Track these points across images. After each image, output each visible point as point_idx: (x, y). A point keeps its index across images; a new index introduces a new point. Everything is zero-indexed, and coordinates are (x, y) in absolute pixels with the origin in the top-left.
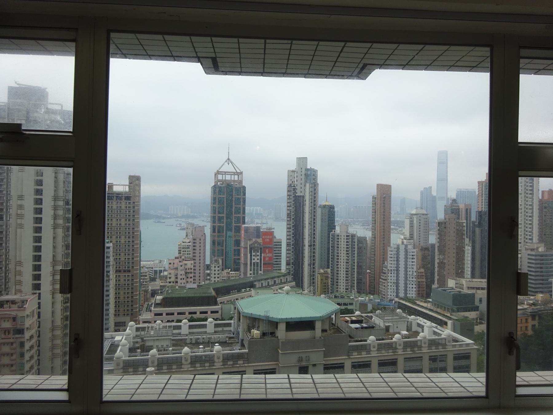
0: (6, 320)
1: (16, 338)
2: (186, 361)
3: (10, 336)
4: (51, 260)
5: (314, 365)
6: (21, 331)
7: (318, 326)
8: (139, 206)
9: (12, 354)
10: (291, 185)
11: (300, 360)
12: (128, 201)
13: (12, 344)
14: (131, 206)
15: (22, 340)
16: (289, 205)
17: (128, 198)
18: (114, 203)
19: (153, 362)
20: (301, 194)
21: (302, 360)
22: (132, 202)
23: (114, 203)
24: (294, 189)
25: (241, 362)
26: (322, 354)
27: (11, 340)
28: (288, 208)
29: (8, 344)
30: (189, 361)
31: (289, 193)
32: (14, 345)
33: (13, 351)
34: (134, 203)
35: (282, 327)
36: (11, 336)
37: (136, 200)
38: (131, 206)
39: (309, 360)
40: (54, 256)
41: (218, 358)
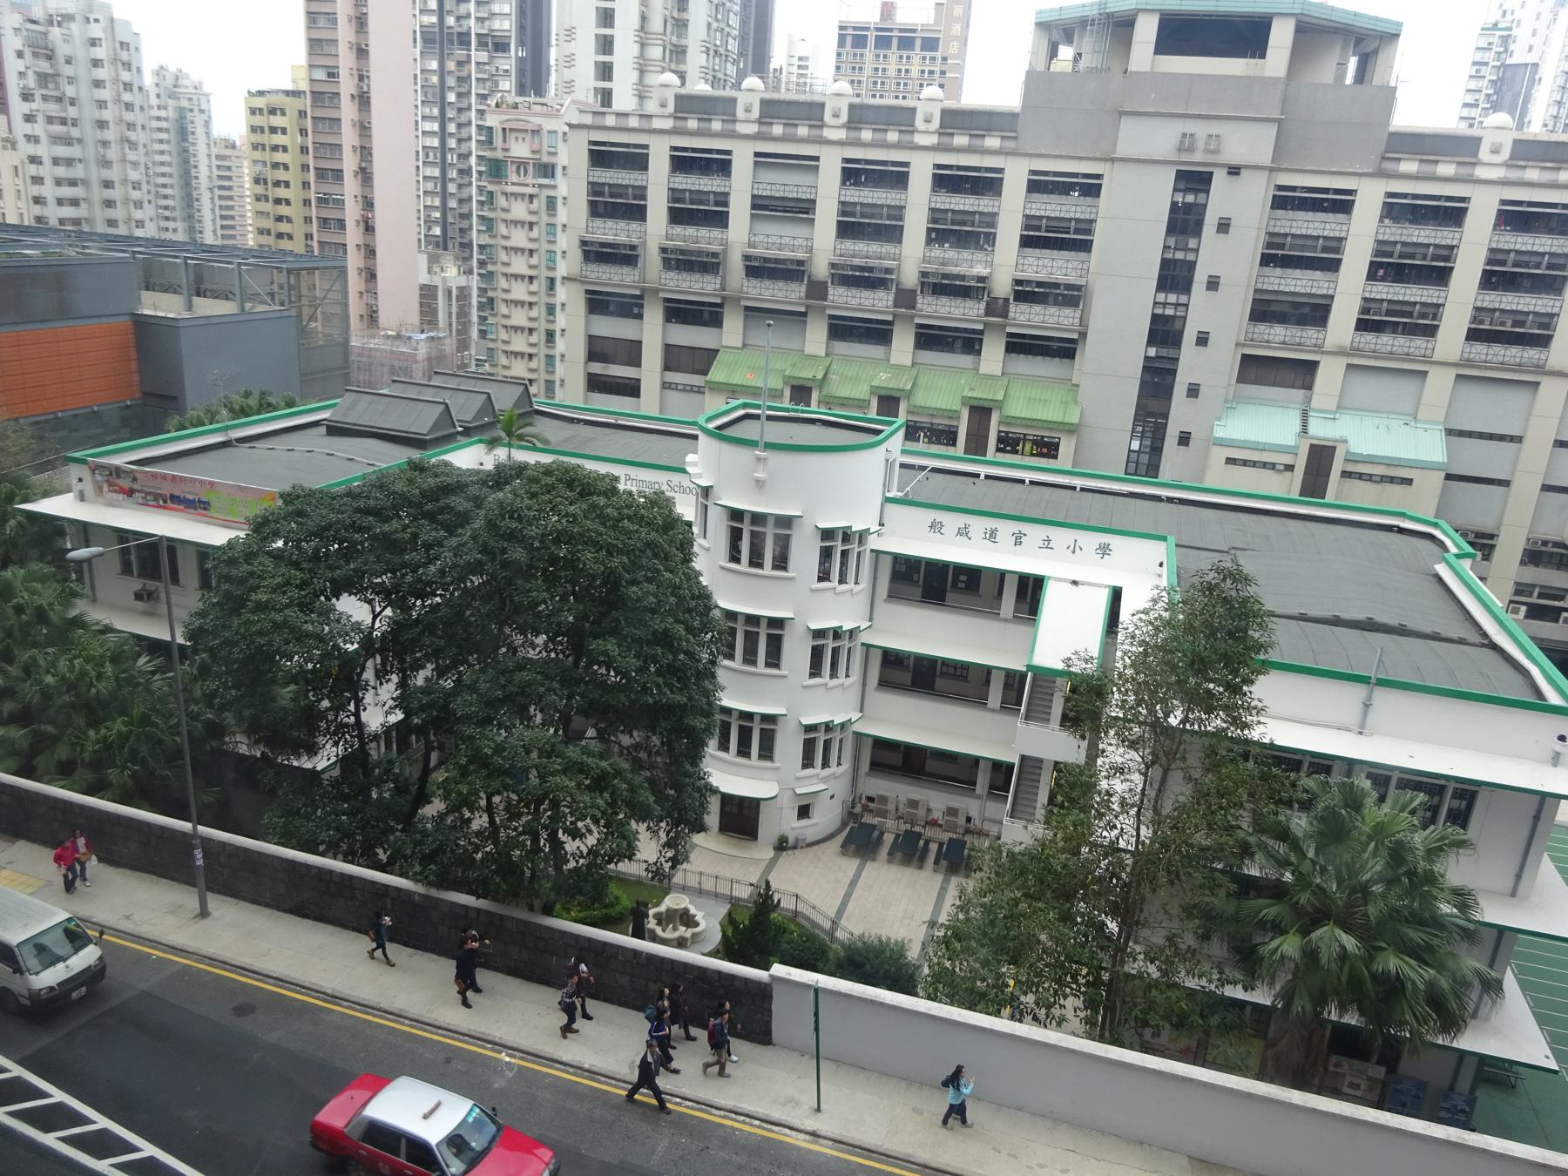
0: (520, 136)
1: (540, 186)
2: (836, 115)
3: (530, 180)
4: (636, 24)
5: (1234, 171)
6: (547, 170)
7: (1281, 36)
8: (960, 68)
9: (531, 225)
10: (1496, 25)
11: (1186, 144)
12: (928, 54)
13: (531, 197)
14: (937, 69)
15: (552, 193)
16: (1470, 99)
17: (930, 44)
18: (893, 59)
19: (748, 111)
20: (1530, 59)
21: (1191, 149)
22: (938, 55)
23: (893, 59)
24: (1505, 40)
25: (992, 142)
26: (1272, 130)
27: (529, 190)
28: (1466, 112)
29: (523, 196)
30: (844, 118)
31: (1479, 57)
32: (535, 206)
33: (533, 219)
34: (944, 59)
35: (1146, 31)
36: (530, 180)
37: (951, 51)
38: (937, 69)
39: (1216, 152)
40: (644, 18)
41: (928, 121)
